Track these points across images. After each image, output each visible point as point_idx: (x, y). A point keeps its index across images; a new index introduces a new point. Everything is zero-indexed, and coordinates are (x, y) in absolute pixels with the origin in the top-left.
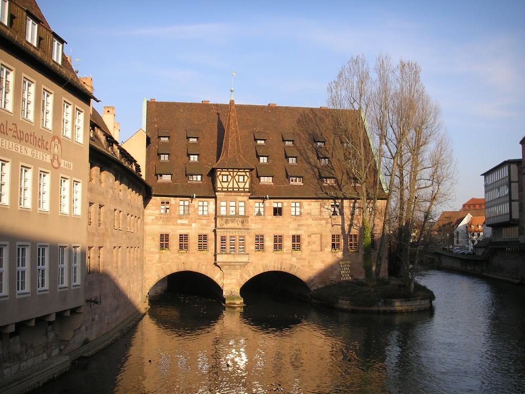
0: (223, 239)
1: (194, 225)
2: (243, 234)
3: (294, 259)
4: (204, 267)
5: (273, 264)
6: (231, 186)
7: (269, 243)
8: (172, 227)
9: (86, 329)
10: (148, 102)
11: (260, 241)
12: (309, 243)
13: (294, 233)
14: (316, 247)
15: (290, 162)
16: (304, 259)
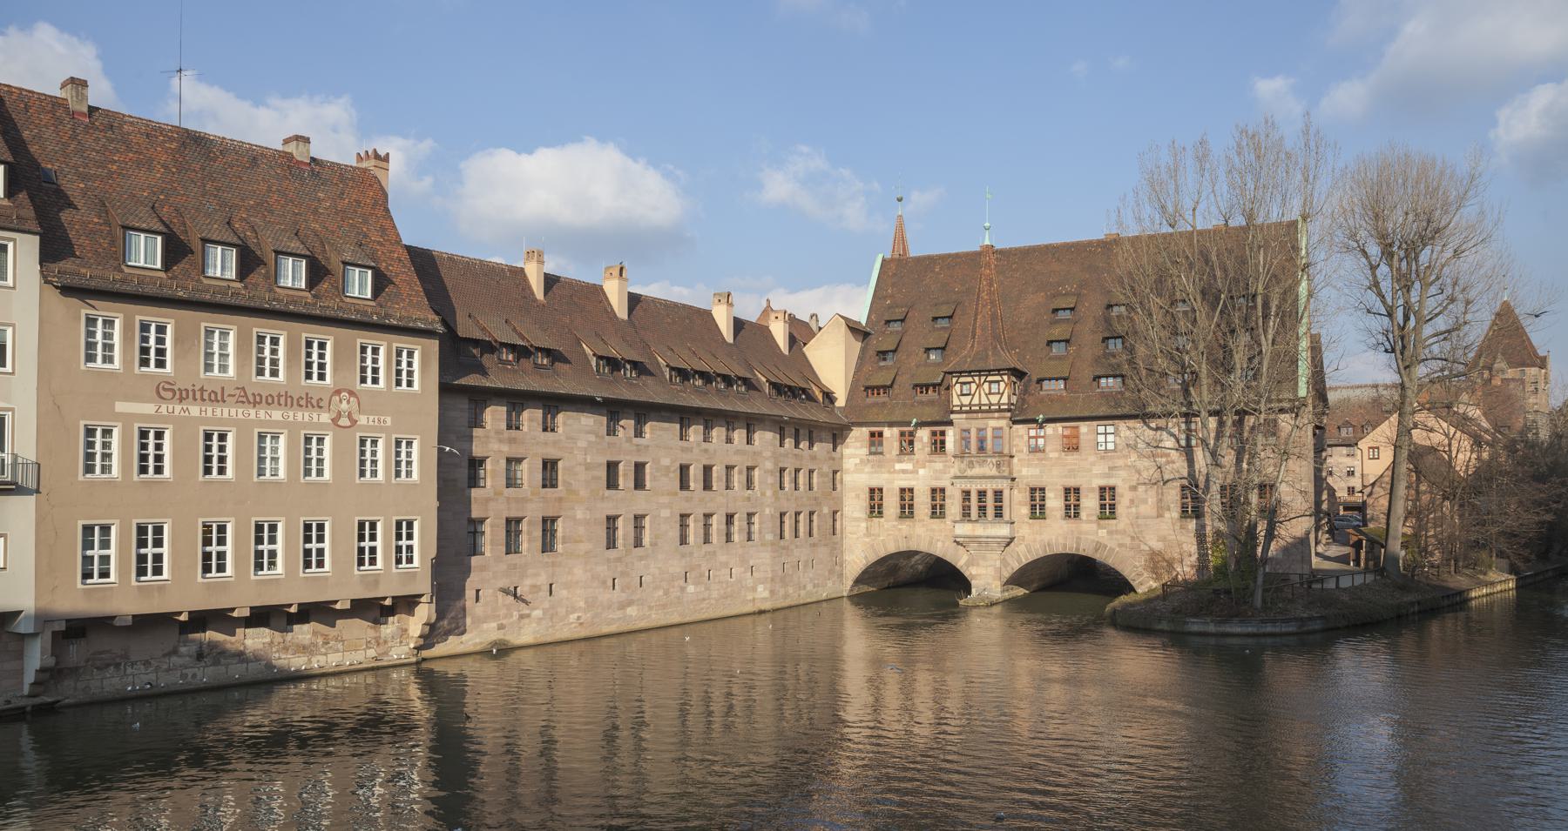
0: (967, 493)
1: (921, 471)
2: (1000, 487)
3: (1103, 533)
4: (939, 544)
5: (1061, 541)
6: (976, 401)
7: (1054, 502)
8: (886, 476)
9: (501, 627)
10: (884, 260)
11: (1037, 497)
12: (1132, 501)
13: (1103, 482)
14: (1148, 508)
15: (1111, 346)
16: (1124, 532)
